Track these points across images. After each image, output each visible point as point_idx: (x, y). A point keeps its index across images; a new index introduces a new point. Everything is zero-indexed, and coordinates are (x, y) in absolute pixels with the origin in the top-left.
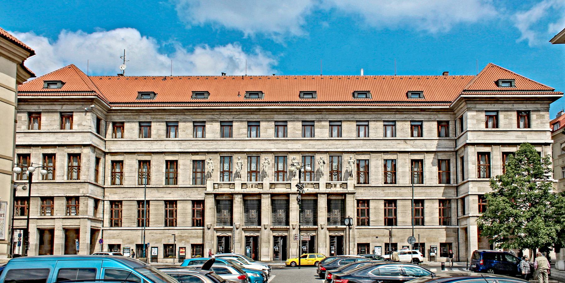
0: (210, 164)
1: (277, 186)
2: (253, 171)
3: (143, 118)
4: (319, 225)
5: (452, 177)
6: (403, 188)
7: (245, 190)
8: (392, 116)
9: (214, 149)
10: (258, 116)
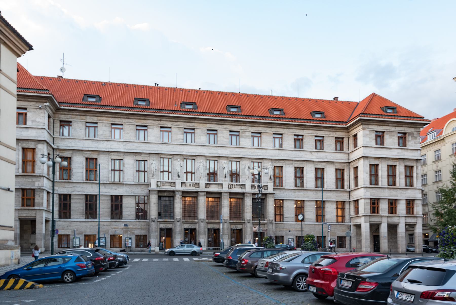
0: (153, 164)
1: (211, 186)
2: (189, 172)
3: (89, 119)
5: (346, 183)
6: (309, 192)
7: (184, 188)
8: (301, 131)
9: (156, 151)
10: (193, 124)
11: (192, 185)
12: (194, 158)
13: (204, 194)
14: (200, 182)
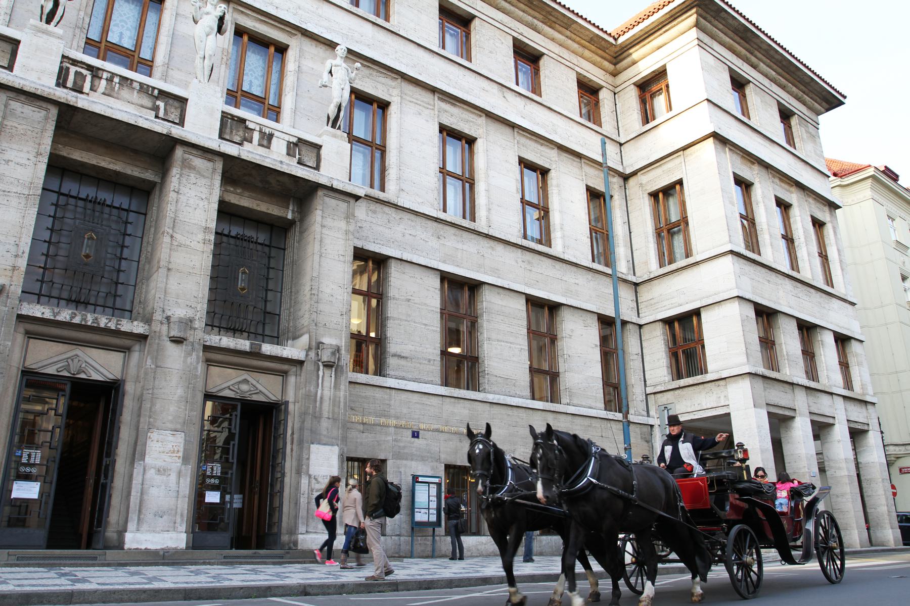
4: (158, 316)
5: (621, 251)
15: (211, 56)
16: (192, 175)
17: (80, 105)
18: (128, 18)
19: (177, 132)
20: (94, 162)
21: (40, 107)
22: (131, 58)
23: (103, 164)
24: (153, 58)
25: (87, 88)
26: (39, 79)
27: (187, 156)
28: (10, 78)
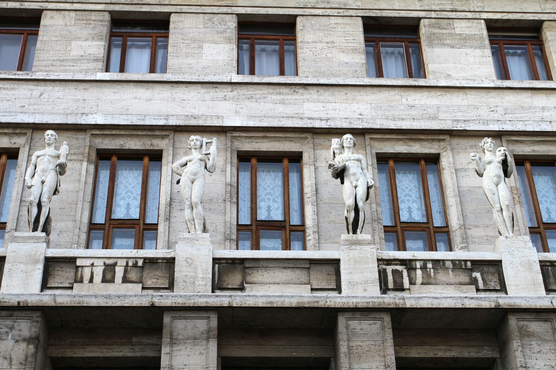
1: (258, 276)
11: (119, 272)
12: (159, 144)
13: (201, 325)
14: (181, 252)
15: (508, 206)
16: (534, 343)
17: (408, 305)
18: (410, 190)
19: (504, 301)
20: (431, 355)
21: (375, 319)
22: (433, 233)
23: (440, 354)
24: (447, 223)
25: (406, 284)
26: (365, 290)
27: (522, 323)
28: (344, 300)
